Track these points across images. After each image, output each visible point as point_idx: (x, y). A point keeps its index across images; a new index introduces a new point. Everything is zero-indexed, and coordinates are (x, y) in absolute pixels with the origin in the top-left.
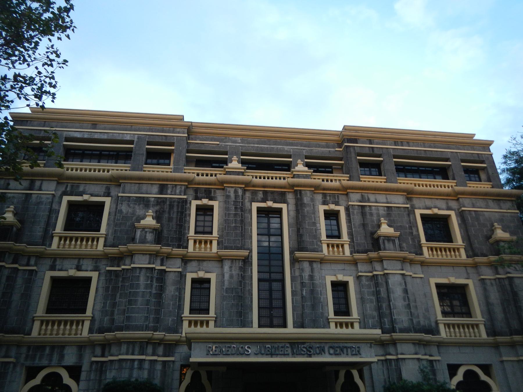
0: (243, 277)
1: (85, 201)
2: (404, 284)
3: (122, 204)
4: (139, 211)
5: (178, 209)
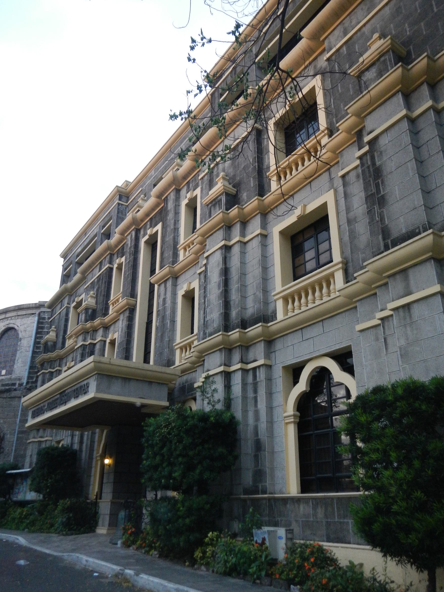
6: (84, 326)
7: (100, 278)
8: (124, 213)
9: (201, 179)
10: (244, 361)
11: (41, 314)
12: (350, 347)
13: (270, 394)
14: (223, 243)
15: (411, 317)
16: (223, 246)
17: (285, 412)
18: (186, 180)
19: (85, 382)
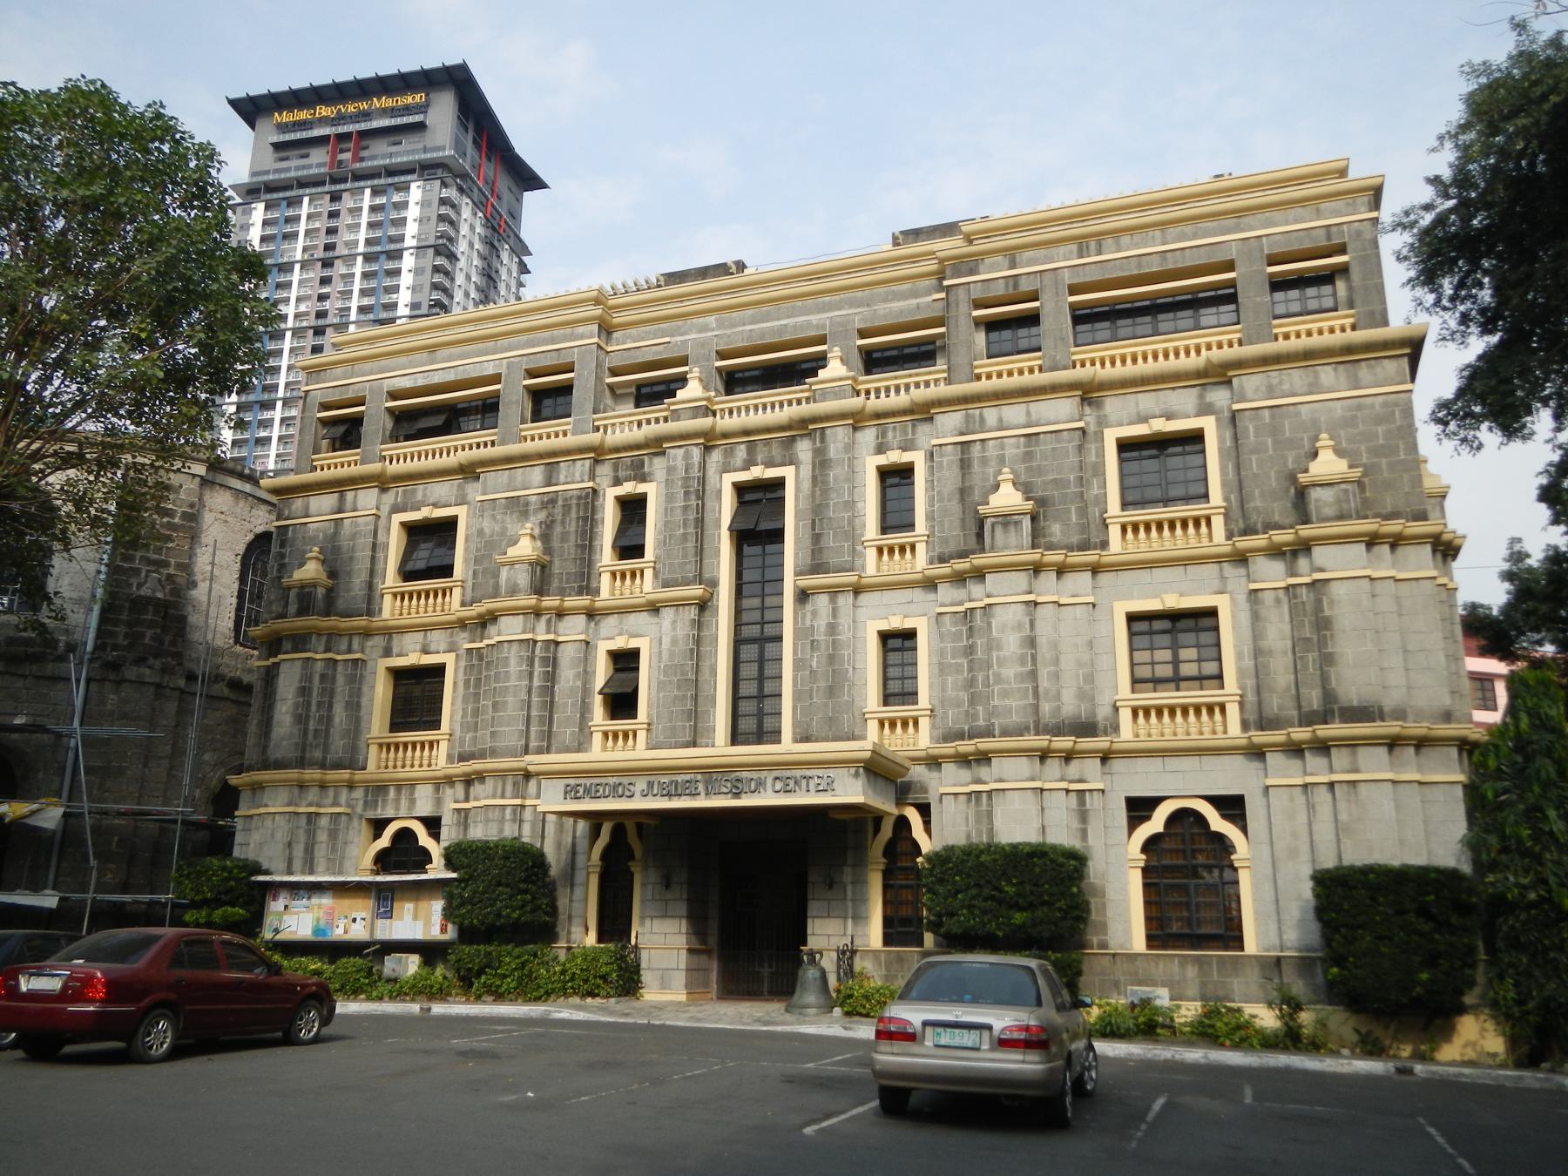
0: (698, 641)
1: (426, 520)
2: (1028, 626)
3: (482, 516)
4: (513, 527)
5: (578, 512)
15: (1356, 793)
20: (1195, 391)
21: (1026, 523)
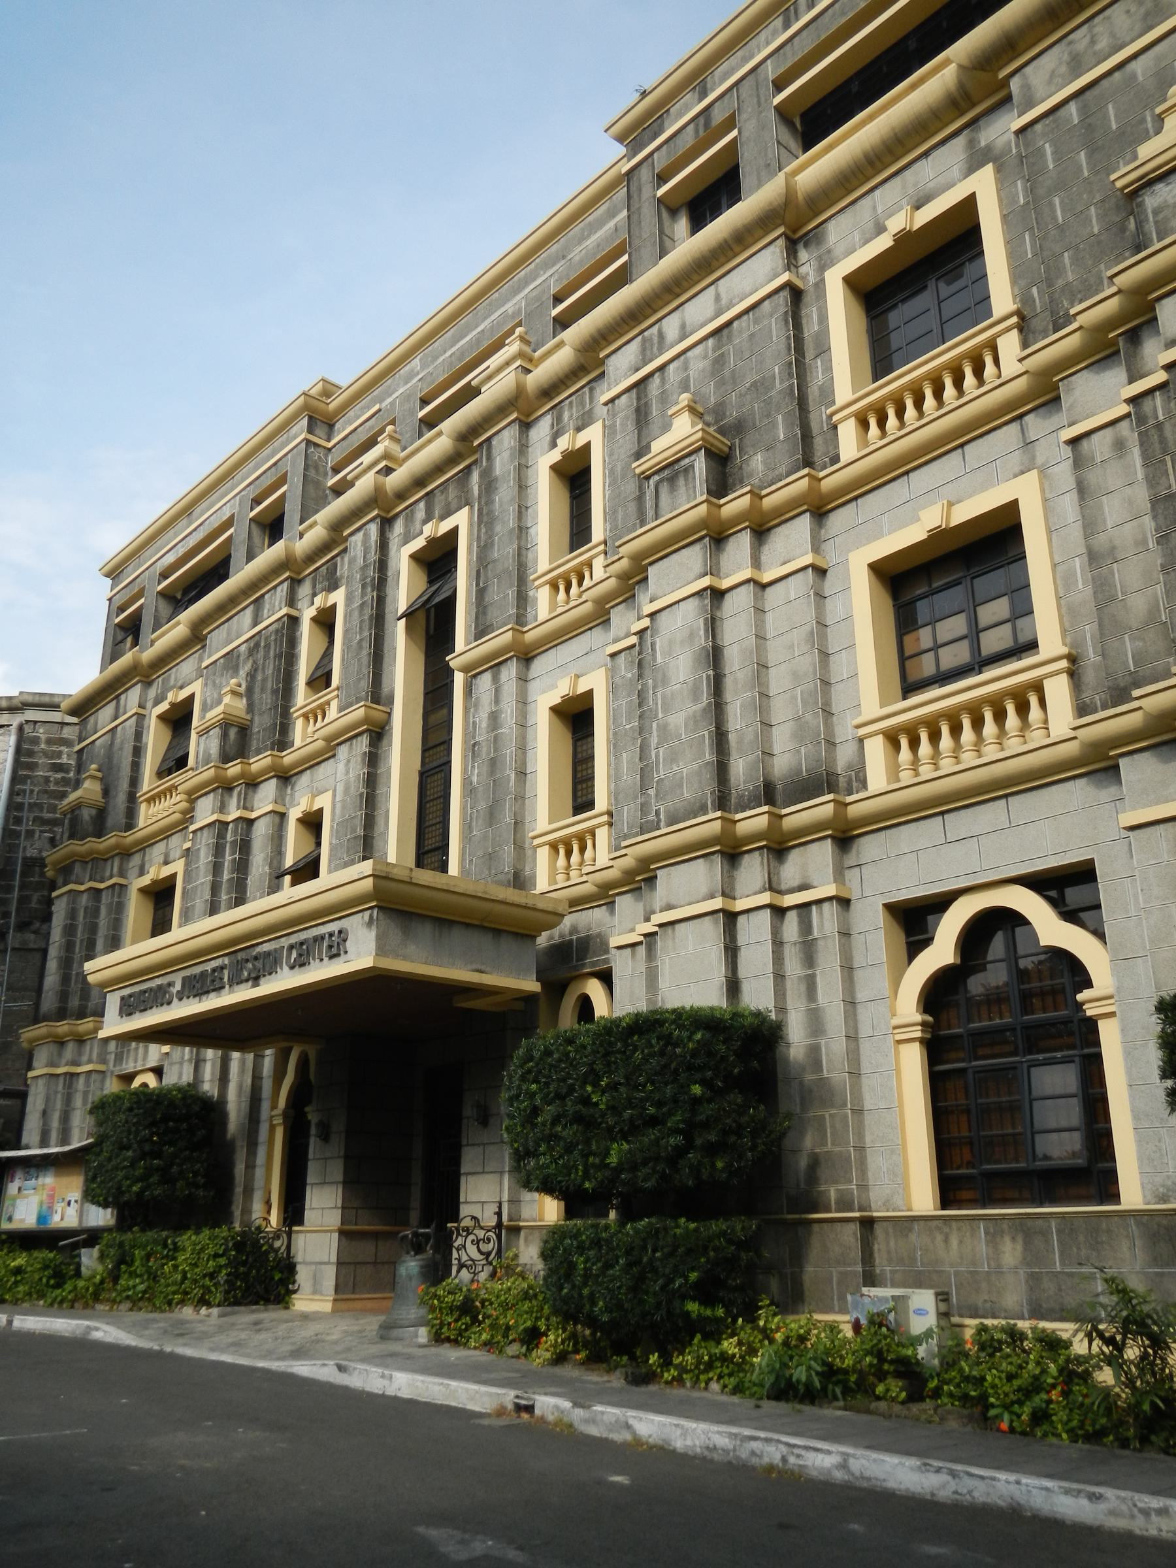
6: (221, 772)
7: (257, 645)
8: (321, 469)
9: (606, 404)
10: (774, 885)
11: (27, 729)
12: (1092, 861)
13: (848, 969)
14: (706, 582)
16: (705, 589)
17: (894, 1015)
18: (551, 399)
19: (334, 927)
20: (960, 142)
21: (700, 464)
